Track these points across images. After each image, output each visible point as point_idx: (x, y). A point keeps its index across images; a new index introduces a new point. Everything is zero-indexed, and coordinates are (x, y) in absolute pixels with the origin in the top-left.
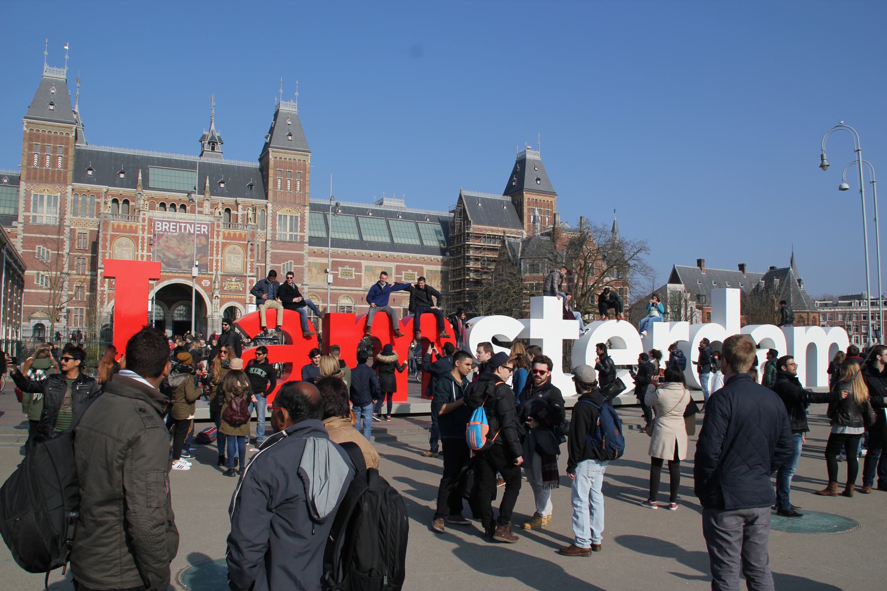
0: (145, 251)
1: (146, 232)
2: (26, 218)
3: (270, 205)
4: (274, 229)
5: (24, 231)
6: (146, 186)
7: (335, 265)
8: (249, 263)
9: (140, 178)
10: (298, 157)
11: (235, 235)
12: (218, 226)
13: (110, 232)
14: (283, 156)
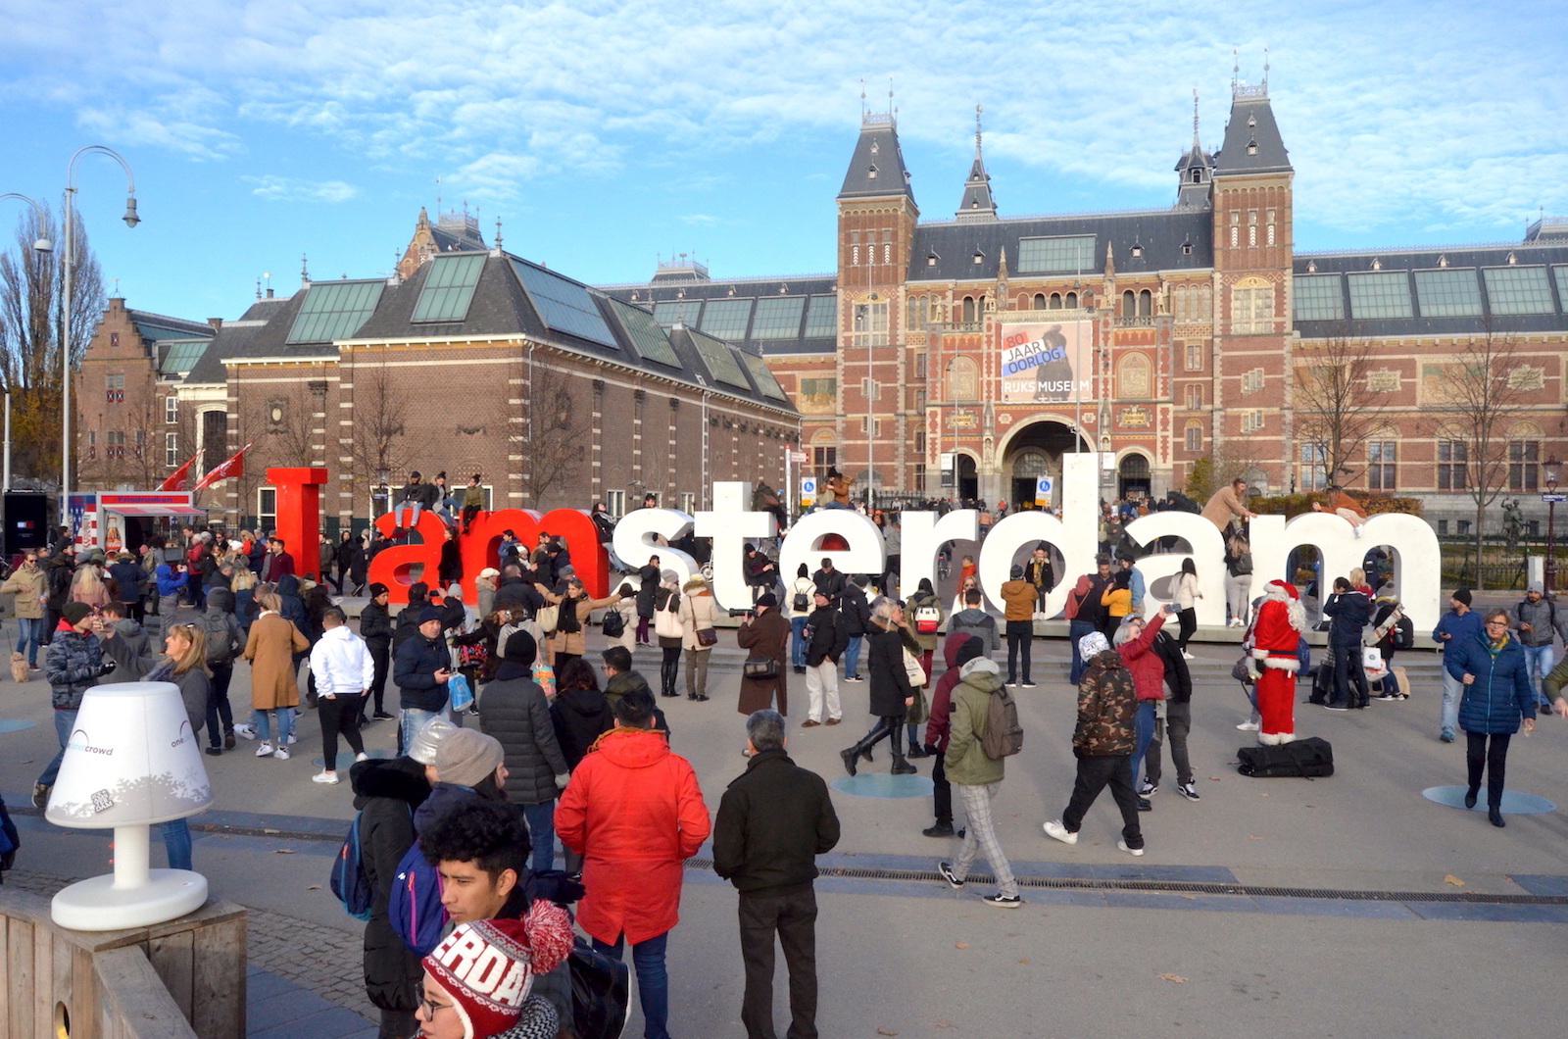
0: (993, 375)
1: (993, 346)
2: (847, 340)
3: (1217, 276)
4: (1226, 315)
5: (845, 359)
6: (1013, 270)
8: (1160, 381)
9: (1003, 260)
10: (1267, 184)
11: (1135, 335)
12: (1106, 324)
13: (942, 351)
14: (1240, 186)
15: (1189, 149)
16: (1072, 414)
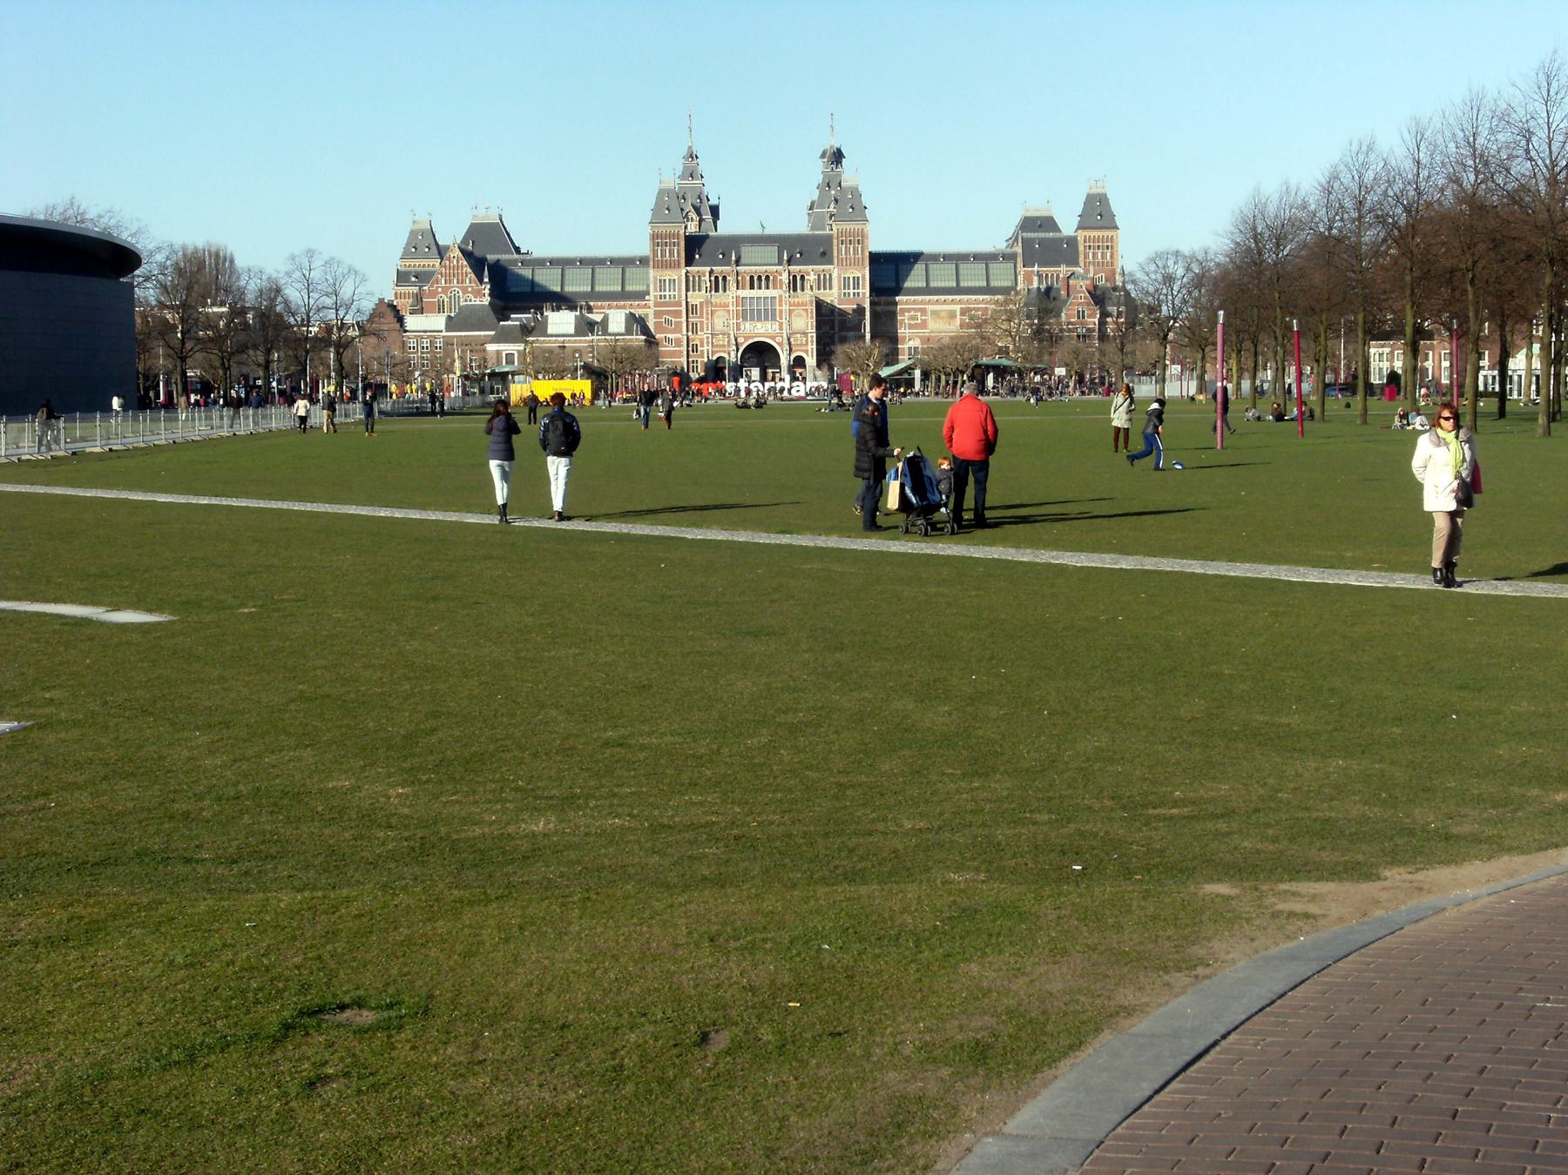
16: (773, 338)
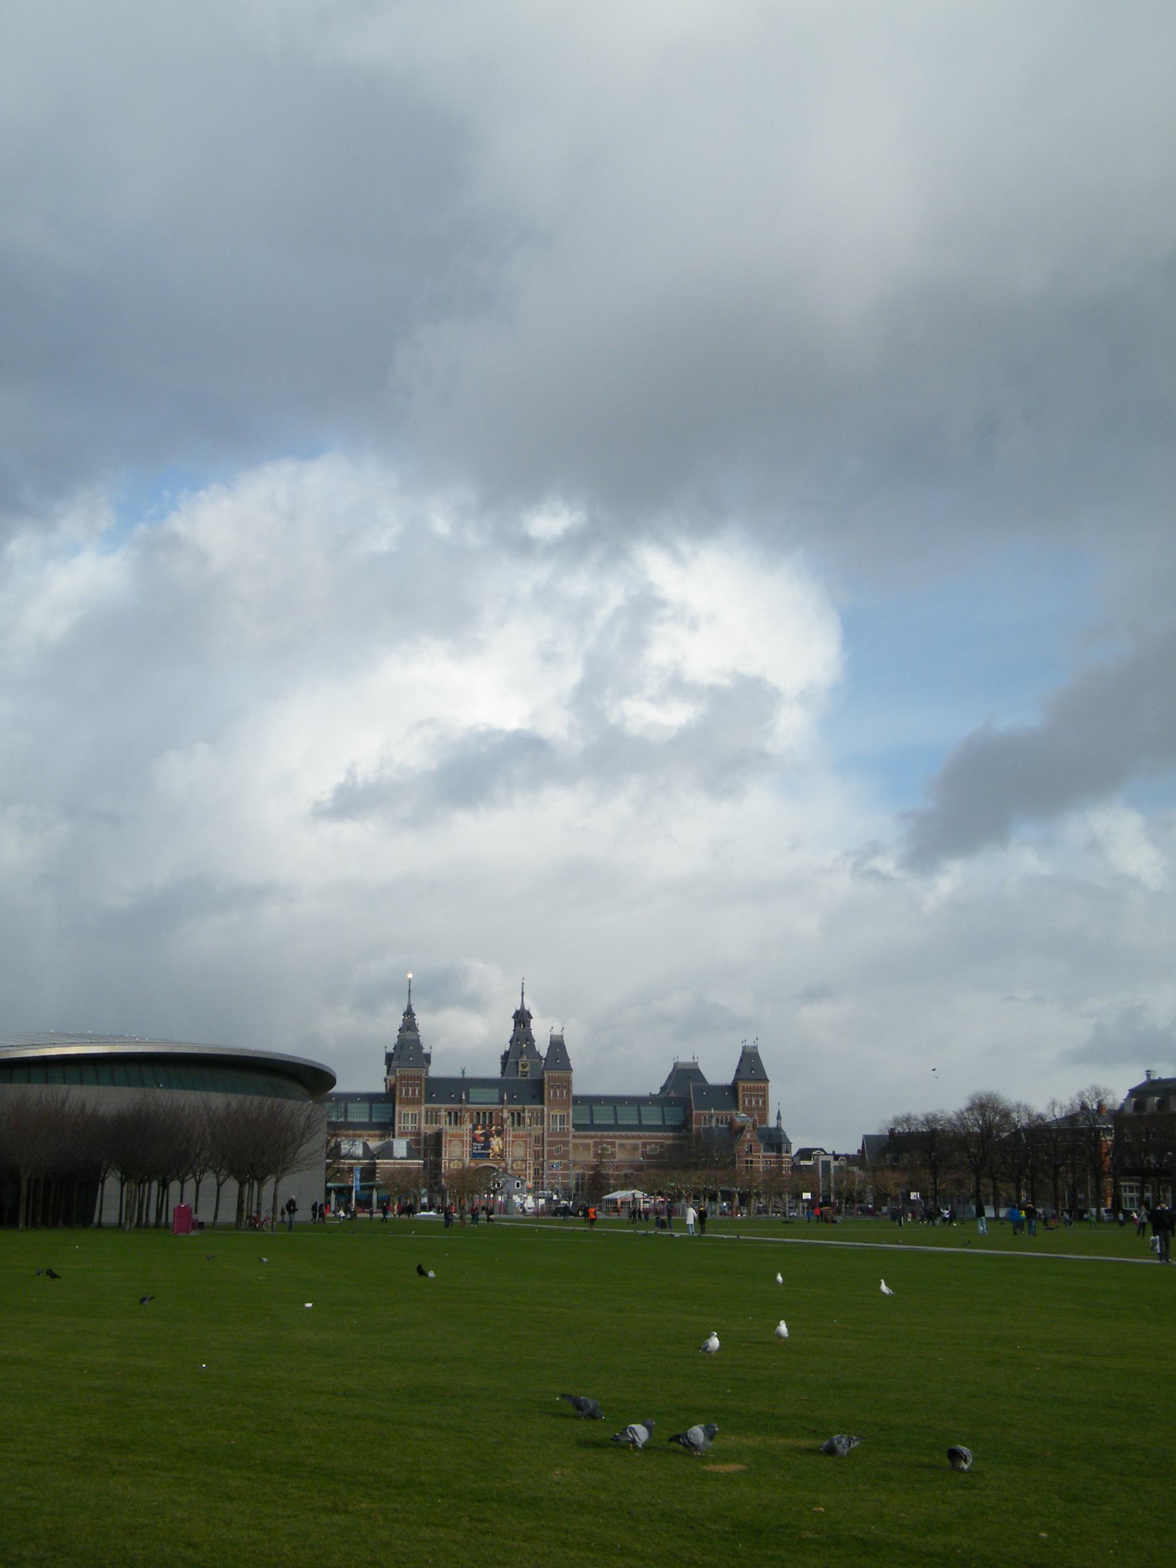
6: (468, 1102)
7: (596, 1145)
15: (519, 1008)
